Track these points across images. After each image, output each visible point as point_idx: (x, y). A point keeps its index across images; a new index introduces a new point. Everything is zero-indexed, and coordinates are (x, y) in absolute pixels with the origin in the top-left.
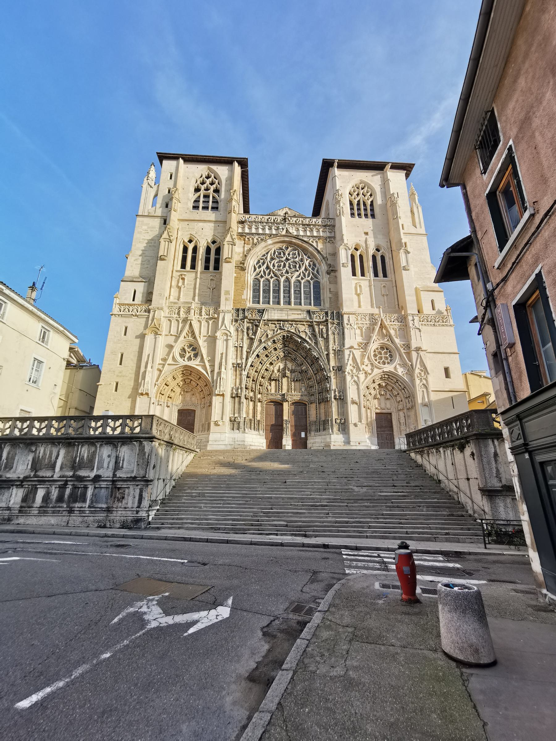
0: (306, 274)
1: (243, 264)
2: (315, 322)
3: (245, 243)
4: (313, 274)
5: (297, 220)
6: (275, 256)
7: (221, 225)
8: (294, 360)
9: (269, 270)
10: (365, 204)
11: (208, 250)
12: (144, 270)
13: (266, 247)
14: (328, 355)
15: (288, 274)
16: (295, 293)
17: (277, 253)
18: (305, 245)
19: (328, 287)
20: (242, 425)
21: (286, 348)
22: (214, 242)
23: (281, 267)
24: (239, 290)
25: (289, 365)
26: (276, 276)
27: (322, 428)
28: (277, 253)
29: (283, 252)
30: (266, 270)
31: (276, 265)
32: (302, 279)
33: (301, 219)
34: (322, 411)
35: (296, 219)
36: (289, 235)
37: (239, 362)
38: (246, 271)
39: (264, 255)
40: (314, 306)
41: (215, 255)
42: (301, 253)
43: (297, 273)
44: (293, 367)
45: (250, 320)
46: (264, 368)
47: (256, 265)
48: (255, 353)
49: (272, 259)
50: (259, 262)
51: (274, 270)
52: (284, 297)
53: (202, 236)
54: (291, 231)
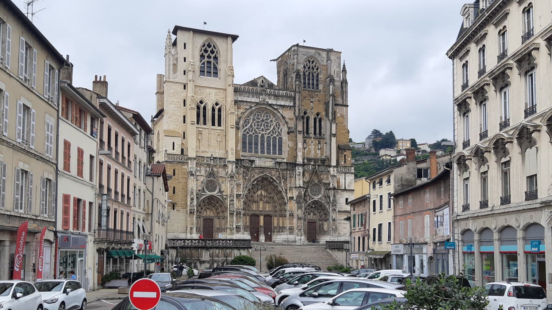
2: (281, 169)
3: (238, 108)
4: (278, 132)
5: (270, 91)
7: (222, 91)
8: (266, 190)
10: (313, 75)
11: (213, 109)
12: (176, 126)
14: (286, 190)
16: (267, 145)
17: (256, 115)
20: (242, 229)
21: (263, 183)
22: (217, 104)
25: (263, 193)
26: (256, 132)
28: (256, 115)
31: (256, 124)
32: (272, 135)
33: (273, 90)
34: (281, 221)
36: (266, 103)
37: (240, 193)
38: (239, 130)
40: (278, 155)
44: (265, 195)
46: (251, 195)
48: (248, 188)
49: (254, 120)
51: (255, 128)
54: (267, 100)
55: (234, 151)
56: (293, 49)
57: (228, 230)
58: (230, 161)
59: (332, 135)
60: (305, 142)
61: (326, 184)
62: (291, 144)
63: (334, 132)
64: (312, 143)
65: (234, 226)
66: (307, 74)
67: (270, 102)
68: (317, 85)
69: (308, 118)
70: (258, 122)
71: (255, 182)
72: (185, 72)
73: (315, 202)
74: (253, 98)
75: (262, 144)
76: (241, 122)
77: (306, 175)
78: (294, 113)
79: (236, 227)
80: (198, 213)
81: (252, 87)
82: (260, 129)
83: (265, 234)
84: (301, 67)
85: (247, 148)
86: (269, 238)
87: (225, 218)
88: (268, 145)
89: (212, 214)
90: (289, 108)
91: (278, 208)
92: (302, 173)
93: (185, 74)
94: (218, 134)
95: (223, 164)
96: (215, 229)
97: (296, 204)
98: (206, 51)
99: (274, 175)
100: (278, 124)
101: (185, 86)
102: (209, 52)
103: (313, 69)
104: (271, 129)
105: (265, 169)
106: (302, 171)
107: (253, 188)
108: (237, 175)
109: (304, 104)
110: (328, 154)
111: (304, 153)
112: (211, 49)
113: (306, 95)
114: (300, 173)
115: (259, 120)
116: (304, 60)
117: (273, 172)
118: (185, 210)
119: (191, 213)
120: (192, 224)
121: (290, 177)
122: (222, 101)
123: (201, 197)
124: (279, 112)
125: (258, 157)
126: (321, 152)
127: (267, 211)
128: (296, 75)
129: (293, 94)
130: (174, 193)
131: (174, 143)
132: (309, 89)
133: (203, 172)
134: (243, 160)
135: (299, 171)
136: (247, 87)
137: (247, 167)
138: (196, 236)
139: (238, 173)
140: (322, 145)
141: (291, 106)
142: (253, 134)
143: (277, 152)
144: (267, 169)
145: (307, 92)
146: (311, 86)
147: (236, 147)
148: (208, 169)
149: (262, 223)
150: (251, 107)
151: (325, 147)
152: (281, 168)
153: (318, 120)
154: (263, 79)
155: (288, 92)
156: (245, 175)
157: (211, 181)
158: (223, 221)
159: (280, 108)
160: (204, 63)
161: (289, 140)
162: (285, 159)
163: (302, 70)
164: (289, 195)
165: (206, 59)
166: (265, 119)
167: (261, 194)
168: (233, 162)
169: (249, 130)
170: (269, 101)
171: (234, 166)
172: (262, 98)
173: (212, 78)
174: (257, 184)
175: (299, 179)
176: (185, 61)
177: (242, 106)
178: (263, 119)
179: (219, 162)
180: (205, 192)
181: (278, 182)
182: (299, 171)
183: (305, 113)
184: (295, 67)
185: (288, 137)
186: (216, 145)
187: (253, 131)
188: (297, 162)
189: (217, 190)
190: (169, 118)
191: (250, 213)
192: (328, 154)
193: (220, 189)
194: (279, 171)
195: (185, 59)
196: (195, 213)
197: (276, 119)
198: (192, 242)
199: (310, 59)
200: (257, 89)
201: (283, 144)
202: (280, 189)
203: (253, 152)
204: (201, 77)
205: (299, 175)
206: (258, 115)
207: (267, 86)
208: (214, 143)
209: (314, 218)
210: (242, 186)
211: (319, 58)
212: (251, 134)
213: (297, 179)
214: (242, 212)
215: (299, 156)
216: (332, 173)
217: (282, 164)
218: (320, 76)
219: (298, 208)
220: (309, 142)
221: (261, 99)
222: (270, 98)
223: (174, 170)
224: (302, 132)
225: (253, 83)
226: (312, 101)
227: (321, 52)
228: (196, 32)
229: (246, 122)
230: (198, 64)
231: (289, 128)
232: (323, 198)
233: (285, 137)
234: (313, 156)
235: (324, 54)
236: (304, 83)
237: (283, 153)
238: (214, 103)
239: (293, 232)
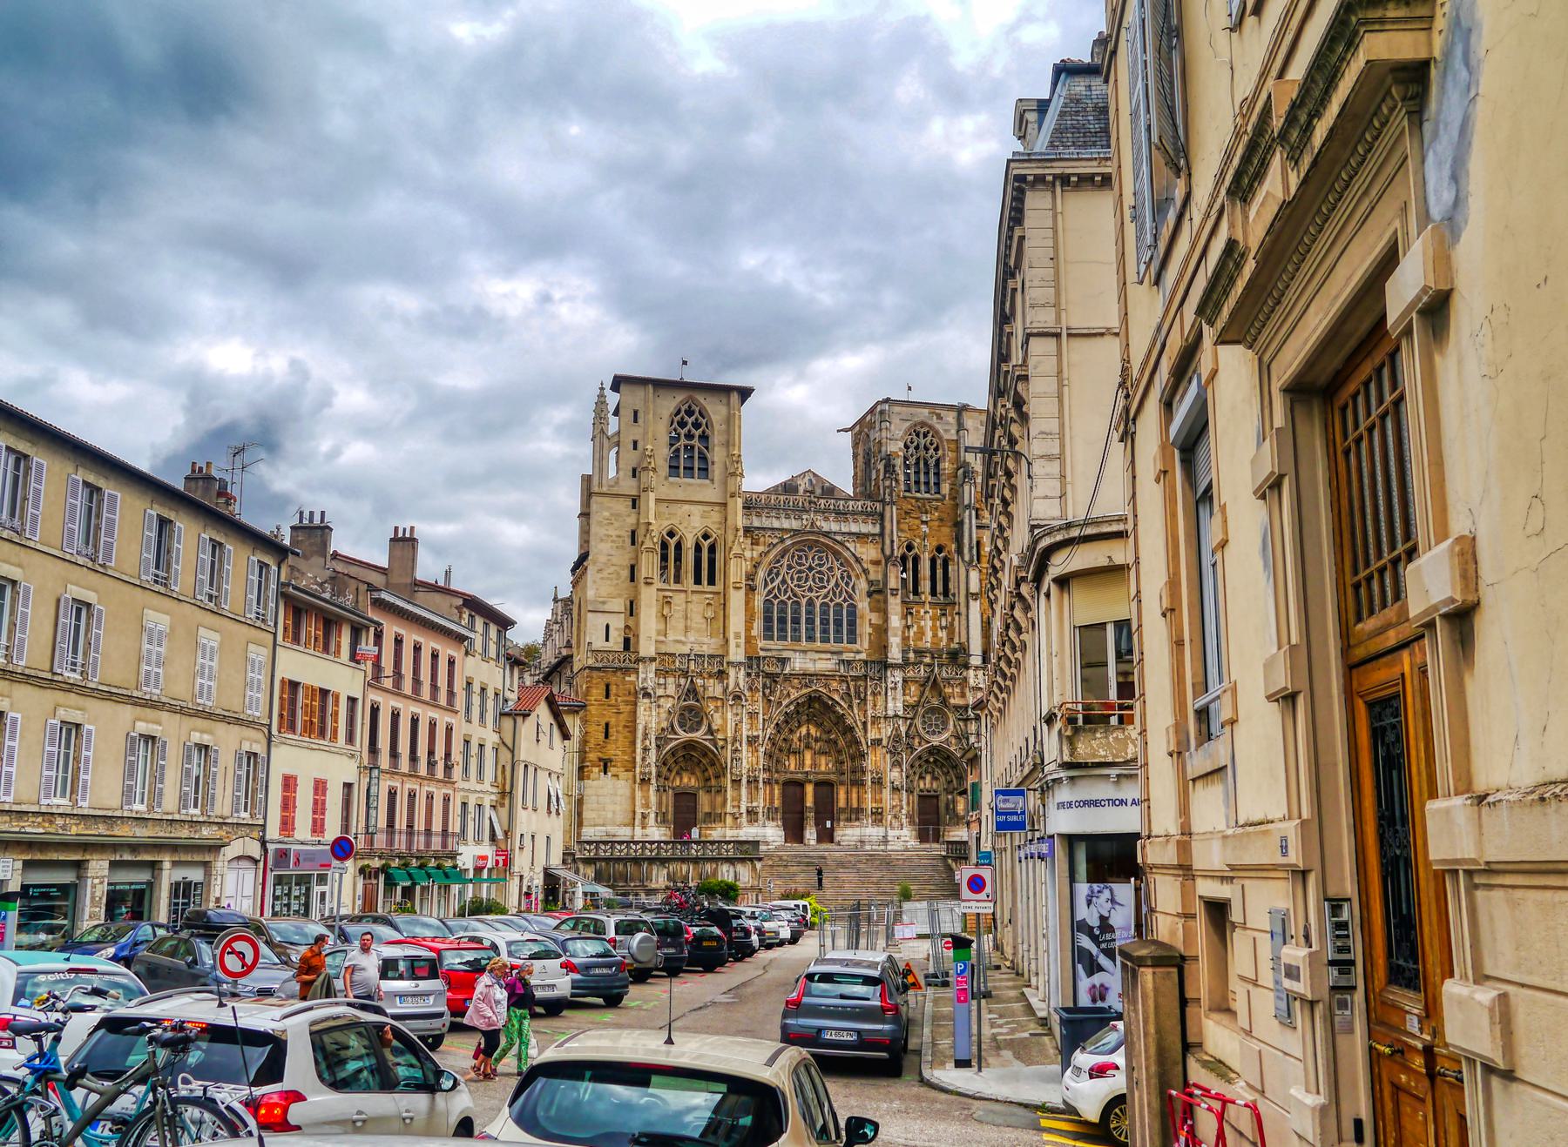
7: (717, 508)
8: (818, 725)
10: (926, 463)
11: (698, 548)
14: (865, 724)
16: (821, 623)
22: (706, 537)
25: (813, 731)
26: (795, 595)
27: (853, 817)
31: (795, 577)
32: (831, 600)
34: (854, 796)
42: (831, 557)
49: (790, 567)
54: (818, 523)
55: (742, 640)
56: (879, 408)
57: (729, 819)
59: (970, 595)
60: (907, 613)
61: (961, 707)
62: (875, 618)
63: (974, 588)
65: (743, 810)
66: (912, 461)
67: (826, 526)
68: (937, 484)
69: (916, 559)
70: (800, 572)
71: (792, 708)
72: (634, 470)
73: (934, 750)
75: (810, 621)
76: (761, 574)
77: (913, 689)
78: (883, 550)
79: (748, 811)
80: (662, 780)
83: (817, 825)
84: (896, 447)
86: (826, 836)
87: (721, 790)
88: (825, 622)
89: (693, 782)
91: (847, 766)
92: (900, 685)
93: (634, 476)
95: (716, 670)
96: (700, 816)
97: (888, 756)
98: (682, 424)
99: (836, 692)
101: (634, 501)
102: (690, 425)
103: (926, 449)
107: (787, 722)
108: (748, 694)
109: (905, 527)
110: (963, 640)
111: (905, 639)
112: (693, 418)
116: (905, 433)
117: (834, 685)
118: (630, 774)
119: (643, 780)
120: (647, 806)
121: (873, 694)
123: (667, 744)
125: (801, 651)
126: (948, 634)
127: (823, 773)
128: (885, 467)
129: (879, 506)
130: (607, 736)
131: (607, 626)
132: (918, 495)
133: (671, 690)
134: (764, 658)
136: (773, 497)
138: (657, 833)
139: (750, 689)
140: (949, 619)
142: (789, 598)
146: (923, 488)
147: (748, 629)
148: (682, 681)
149: (809, 802)
150: (782, 541)
151: (956, 623)
153: (939, 562)
155: (869, 503)
156: (767, 691)
157: (690, 709)
158: (719, 799)
160: (678, 450)
161: (871, 611)
163: (901, 454)
164: (872, 735)
165: (683, 441)
167: (808, 733)
169: (779, 589)
171: (742, 672)
173: (696, 481)
174: (798, 713)
175: (894, 699)
176: (635, 448)
179: (709, 663)
180: (676, 733)
181: (845, 706)
183: (910, 547)
184: (883, 449)
187: (789, 593)
189: (704, 728)
190: (600, 571)
191: (783, 778)
192: (963, 640)
193: (710, 726)
195: (635, 443)
196: (653, 781)
197: (841, 564)
198: (628, 847)
199: (918, 428)
202: (849, 721)
204: (671, 479)
205: (895, 688)
206: (800, 558)
207: (818, 491)
208: (697, 620)
209: (935, 785)
210: (761, 716)
211: (939, 427)
212: (784, 598)
213: (890, 698)
214: (762, 776)
215: (894, 645)
216: (972, 682)
219: (893, 765)
220: (918, 612)
222: (826, 519)
223: (608, 686)
225: (788, 488)
227: (943, 413)
228: (660, 385)
229: (772, 573)
230: (663, 453)
231: (871, 583)
232: (953, 741)
233: (863, 605)
234: (929, 645)
235: (951, 417)
239: (881, 821)
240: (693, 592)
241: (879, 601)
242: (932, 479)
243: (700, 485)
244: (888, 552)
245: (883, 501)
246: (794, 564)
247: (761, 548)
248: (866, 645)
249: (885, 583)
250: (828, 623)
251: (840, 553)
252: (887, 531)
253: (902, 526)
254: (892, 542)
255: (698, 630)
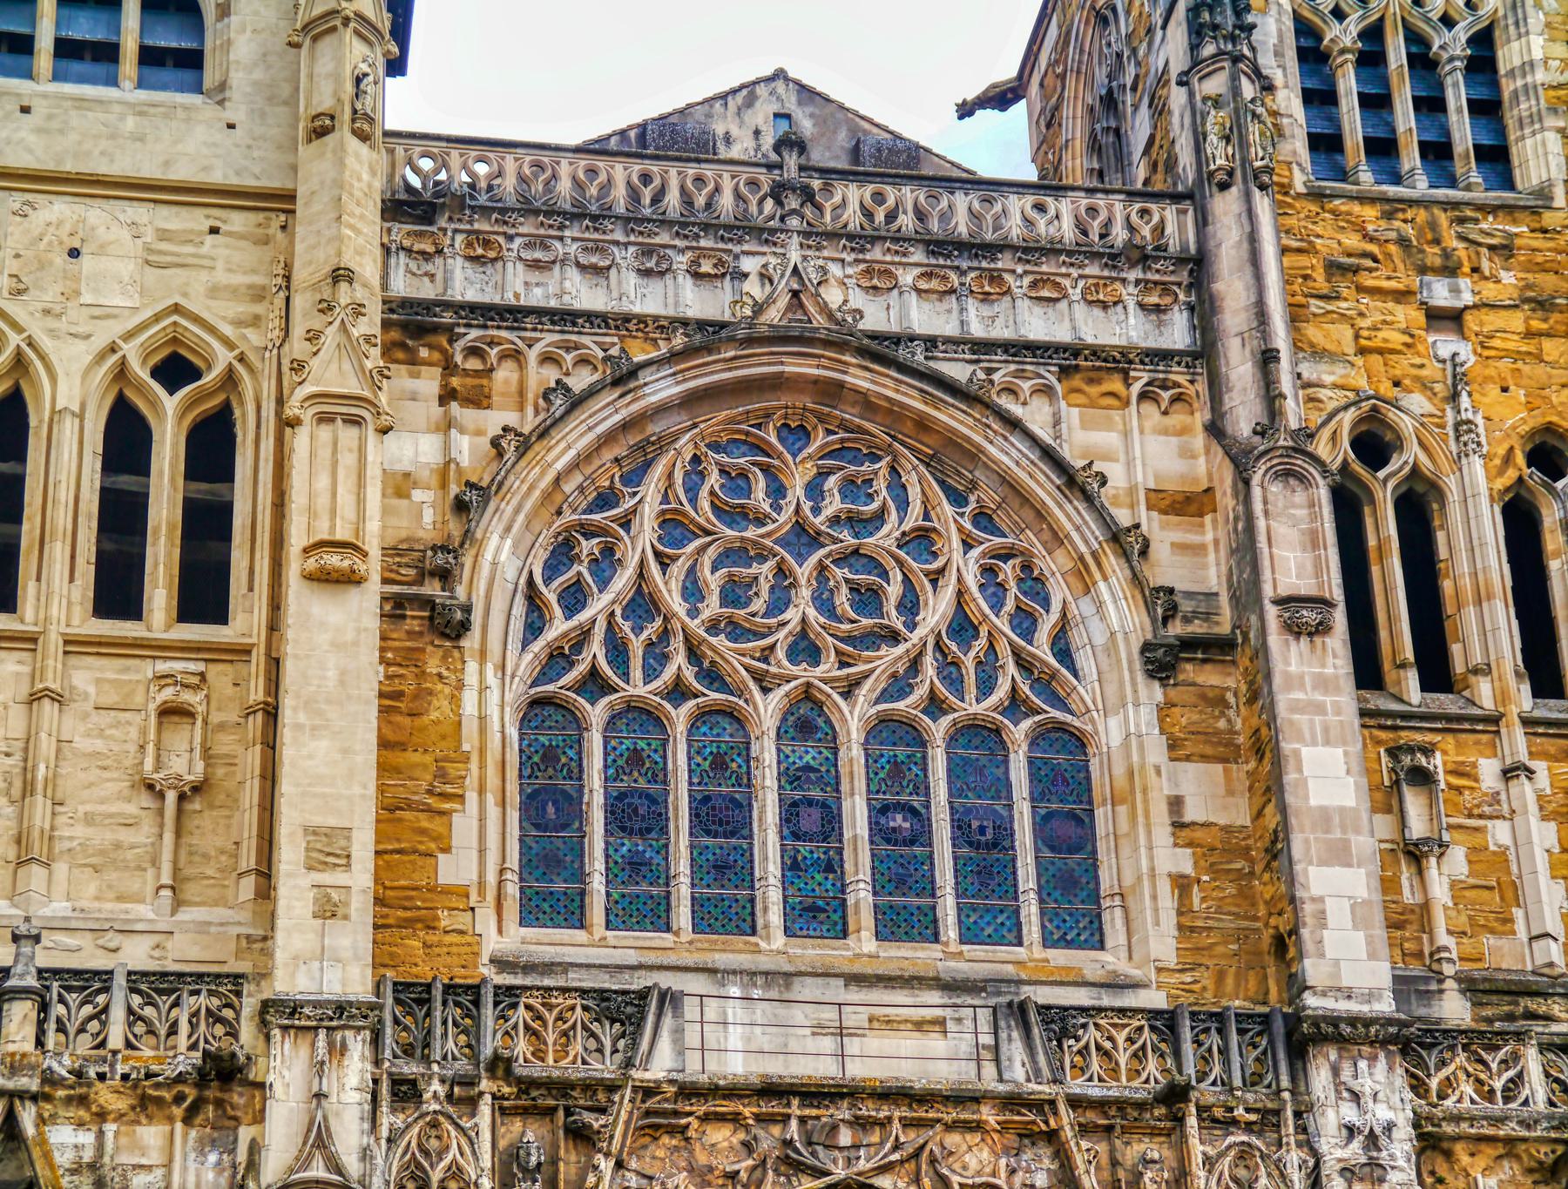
0: (969, 662)
1: (445, 576)
2: (1075, 1102)
5: (879, 198)
6: (705, 504)
7: (238, 221)
9: (652, 629)
10: (1423, 61)
13: (626, 426)
15: (816, 662)
16: (880, 833)
17: (714, 479)
18: (953, 418)
19: (1161, 790)
23: (758, 605)
24: (410, 806)
26: (712, 676)
28: (714, 479)
29: (766, 469)
30: (626, 627)
31: (713, 581)
32: (935, 706)
33: (909, 195)
35: (870, 189)
36: (819, 320)
38: (471, 642)
39: (605, 500)
40: (1047, 943)
41: (191, 474)
43: (890, 656)
45: (527, 1085)
47: (548, 581)
49: (674, 526)
50: (563, 552)
51: (694, 625)
52: (792, 866)
53: (73, 313)
54: (833, 296)
55: (360, 877)
58: (295, 1009)
64: (1525, 792)
67: (876, 316)
68: (1495, 157)
74: (655, 287)
78: (1216, 430)
81: (637, 167)
82: (771, 631)
85: (597, 865)
90: (1141, 377)
92: (1400, 1148)
94: (168, 693)
95: (185, 1060)
100: (1008, 571)
104: (915, 637)
105: (843, 1112)
106: (1403, 1119)
113: (1352, 241)
114: (1372, 1140)
115: (751, 533)
122: (238, 323)
124: (1014, 424)
125: (750, 975)
129: (1177, 226)
132: (1391, 190)
134: (506, 996)
135: (1349, 1113)
137: (562, 1088)
141: (1165, 356)
142: (678, 692)
143: (1030, 910)
144: (867, 1109)
145: (1370, 213)
146: (1410, 158)
150: (624, 377)
152: (1077, 1086)
154: (791, 105)
159: (1026, 386)
161: (1174, 745)
162: (1135, 986)
166: (835, 521)
168: (341, 1008)
169: (617, 650)
170: (858, 299)
171: (356, 1068)
172: (765, 277)
177: (505, 374)
178: (800, 527)
182: (1349, 1113)
185: (1164, 710)
186: (126, 836)
188: (1310, 1000)
194: (1052, 1136)
197: (983, 519)
200: (699, 180)
201: (1099, 813)
203: (683, 916)
206: (737, 480)
212: (638, 688)
215: (1338, 913)
217: (1091, 1035)
218: (1508, 56)
221: (753, 288)
222: (878, 281)
224: (1340, 618)
226: (1440, 293)
236: (1326, 144)
237: (1114, 931)
238: (132, 351)
240: (75, 645)
241: (1217, 701)
242: (1463, 132)
243: (140, 111)
244: (1244, 416)
245: (1192, 198)
246: (704, 512)
247: (495, 419)
248: (1163, 944)
249: (1246, 593)
250: (921, 834)
251: (973, 455)
252: (1234, 316)
253: (1312, 332)
254: (1268, 358)
255: (102, 862)
